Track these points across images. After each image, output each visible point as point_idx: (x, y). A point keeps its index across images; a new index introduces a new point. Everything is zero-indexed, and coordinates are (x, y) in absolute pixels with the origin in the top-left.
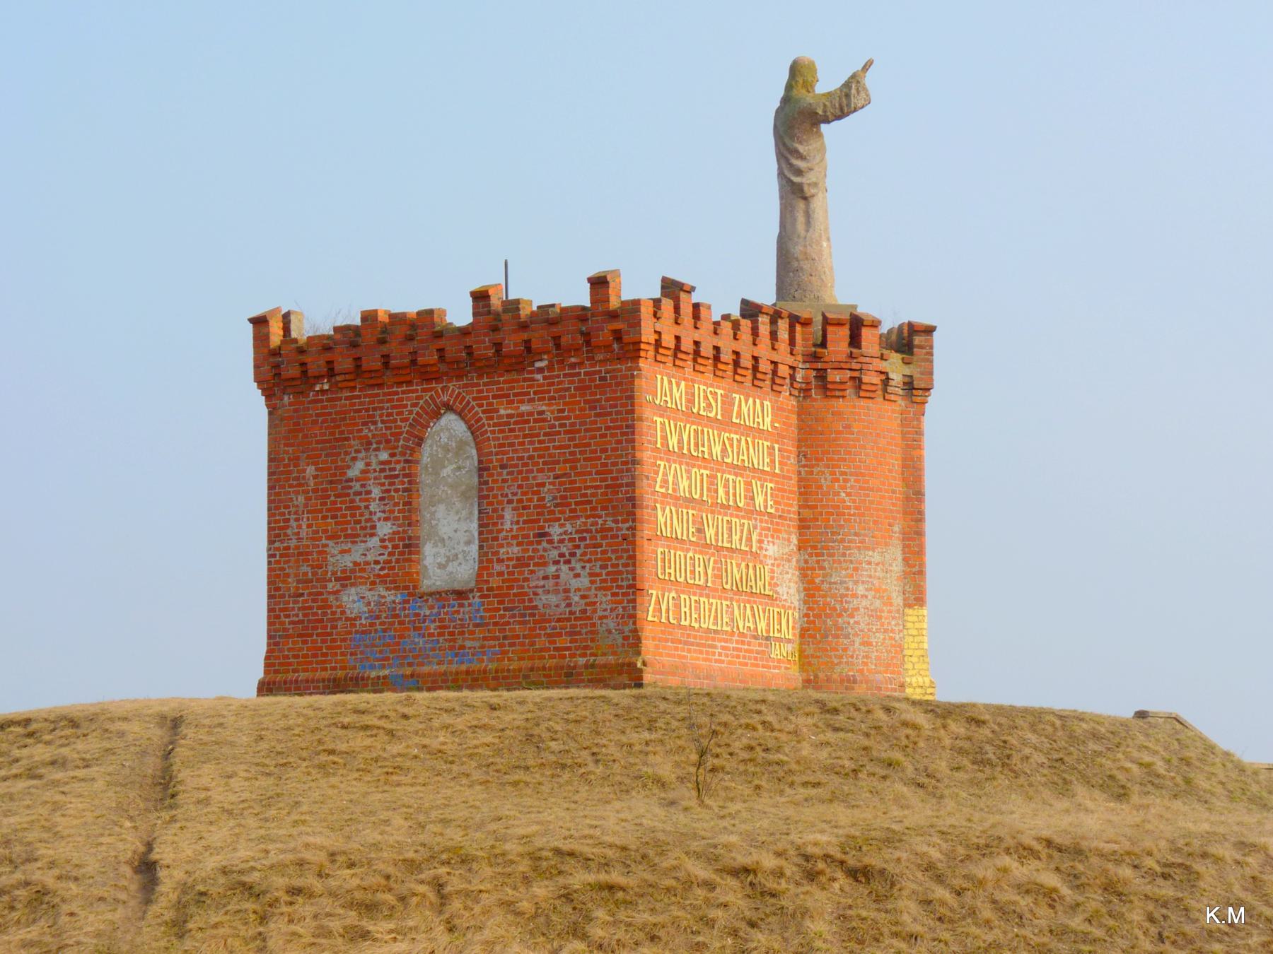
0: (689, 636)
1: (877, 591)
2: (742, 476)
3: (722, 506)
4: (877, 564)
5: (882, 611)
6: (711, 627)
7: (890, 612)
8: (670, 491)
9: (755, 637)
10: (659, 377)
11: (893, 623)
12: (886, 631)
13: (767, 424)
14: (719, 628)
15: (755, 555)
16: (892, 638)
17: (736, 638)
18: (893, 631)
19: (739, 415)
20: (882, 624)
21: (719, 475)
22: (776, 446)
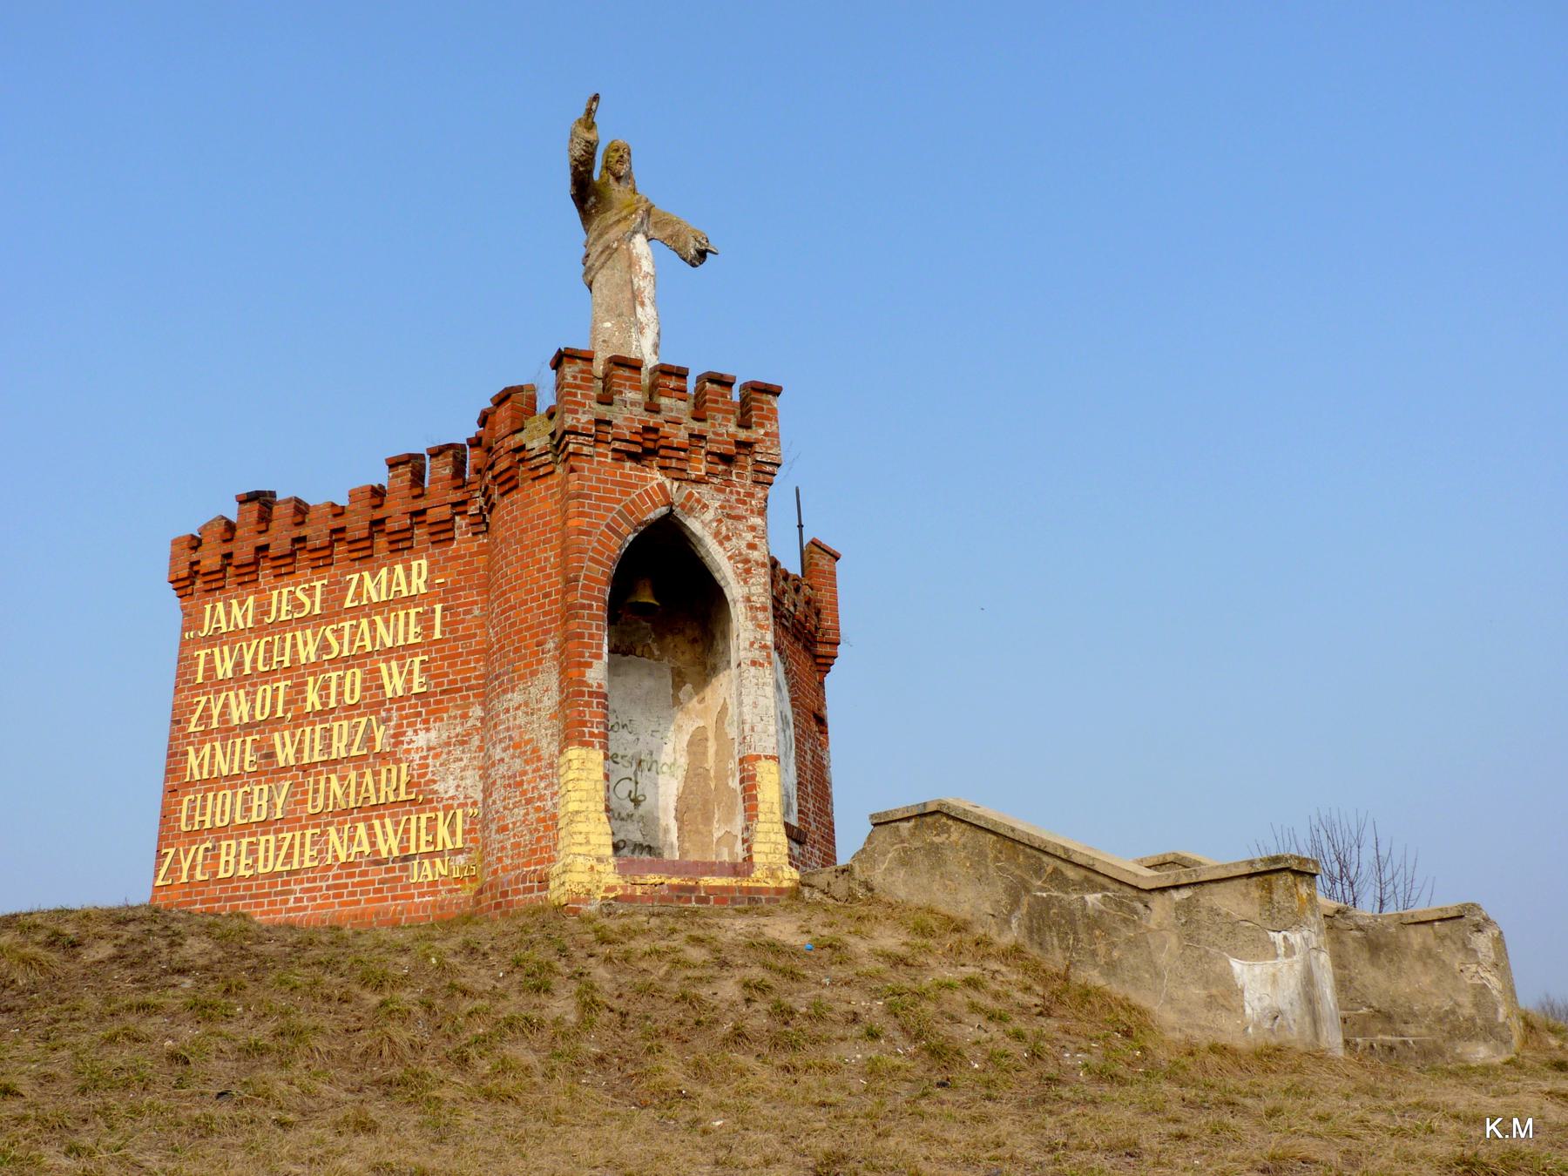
0: (237, 889)
1: (517, 746)
2: (360, 666)
3: (318, 713)
4: (517, 708)
5: (525, 773)
6: (278, 868)
7: (537, 770)
8: (215, 725)
9: (378, 863)
10: (208, 607)
11: (543, 785)
12: (529, 801)
13: (419, 585)
14: (296, 866)
15: (382, 756)
16: (538, 809)
17: (335, 871)
18: (541, 798)
19: (358, 595)
20: (524, 793)
21: (311, 679)
22: (438, 607)
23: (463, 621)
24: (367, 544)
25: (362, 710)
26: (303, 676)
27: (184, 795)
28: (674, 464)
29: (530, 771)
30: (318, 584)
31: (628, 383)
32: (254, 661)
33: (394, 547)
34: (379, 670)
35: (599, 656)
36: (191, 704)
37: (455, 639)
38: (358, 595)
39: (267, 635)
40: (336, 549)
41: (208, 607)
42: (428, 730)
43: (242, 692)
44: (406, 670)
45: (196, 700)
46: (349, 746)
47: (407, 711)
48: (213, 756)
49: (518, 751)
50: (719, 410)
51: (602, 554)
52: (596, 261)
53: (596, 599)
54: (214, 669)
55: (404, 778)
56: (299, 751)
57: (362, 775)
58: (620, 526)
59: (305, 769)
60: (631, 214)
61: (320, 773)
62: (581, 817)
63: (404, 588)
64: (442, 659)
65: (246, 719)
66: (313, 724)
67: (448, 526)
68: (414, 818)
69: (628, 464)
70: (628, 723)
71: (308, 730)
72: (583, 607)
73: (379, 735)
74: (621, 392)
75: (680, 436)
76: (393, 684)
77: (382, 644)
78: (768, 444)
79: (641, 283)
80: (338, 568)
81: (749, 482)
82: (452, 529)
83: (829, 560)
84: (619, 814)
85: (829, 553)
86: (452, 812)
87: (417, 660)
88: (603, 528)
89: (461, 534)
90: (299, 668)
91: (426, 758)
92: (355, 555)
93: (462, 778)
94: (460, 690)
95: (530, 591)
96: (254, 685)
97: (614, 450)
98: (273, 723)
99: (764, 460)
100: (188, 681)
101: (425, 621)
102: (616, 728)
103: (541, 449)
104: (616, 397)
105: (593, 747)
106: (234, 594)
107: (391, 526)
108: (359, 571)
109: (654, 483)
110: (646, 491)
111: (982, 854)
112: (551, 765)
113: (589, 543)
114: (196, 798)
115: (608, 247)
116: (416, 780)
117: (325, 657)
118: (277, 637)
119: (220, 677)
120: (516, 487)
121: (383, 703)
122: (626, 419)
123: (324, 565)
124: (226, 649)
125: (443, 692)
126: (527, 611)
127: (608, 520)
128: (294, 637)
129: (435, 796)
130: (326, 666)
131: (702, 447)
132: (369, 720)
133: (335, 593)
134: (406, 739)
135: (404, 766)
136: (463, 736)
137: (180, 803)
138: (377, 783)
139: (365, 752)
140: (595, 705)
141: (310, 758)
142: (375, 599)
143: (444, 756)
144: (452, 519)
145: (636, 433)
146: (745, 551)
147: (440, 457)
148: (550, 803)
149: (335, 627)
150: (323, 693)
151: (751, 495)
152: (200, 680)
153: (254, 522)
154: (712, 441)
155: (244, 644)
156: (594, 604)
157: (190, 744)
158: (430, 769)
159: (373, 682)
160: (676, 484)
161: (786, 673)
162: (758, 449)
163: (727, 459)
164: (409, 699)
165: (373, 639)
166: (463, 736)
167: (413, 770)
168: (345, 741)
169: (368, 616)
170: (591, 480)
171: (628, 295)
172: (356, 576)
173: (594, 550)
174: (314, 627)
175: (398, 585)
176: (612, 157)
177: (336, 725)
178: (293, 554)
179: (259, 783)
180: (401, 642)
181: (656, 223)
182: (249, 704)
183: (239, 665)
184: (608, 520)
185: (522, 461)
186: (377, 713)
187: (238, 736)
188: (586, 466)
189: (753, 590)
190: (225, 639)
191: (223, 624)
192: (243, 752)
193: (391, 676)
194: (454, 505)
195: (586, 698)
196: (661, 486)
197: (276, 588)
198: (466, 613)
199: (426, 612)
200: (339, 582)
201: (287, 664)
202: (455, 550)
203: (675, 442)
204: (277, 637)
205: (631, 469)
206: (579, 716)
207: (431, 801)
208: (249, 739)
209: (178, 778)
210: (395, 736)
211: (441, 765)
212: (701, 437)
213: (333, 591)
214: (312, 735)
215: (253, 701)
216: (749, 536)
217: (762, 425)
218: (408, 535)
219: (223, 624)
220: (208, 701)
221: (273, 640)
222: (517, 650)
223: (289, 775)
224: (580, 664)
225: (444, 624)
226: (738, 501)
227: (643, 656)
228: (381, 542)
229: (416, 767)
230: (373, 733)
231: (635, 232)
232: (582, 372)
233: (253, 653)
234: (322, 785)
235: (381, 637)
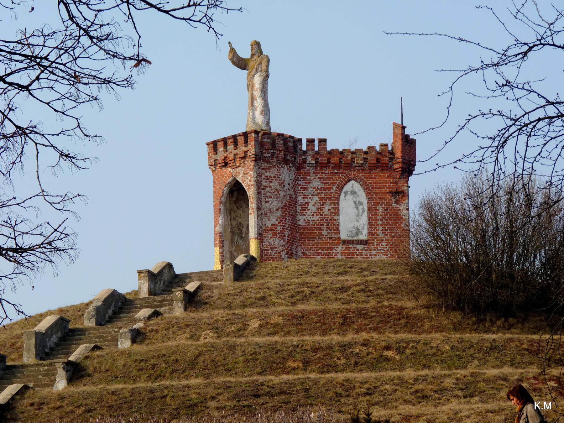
51: (218, 196)
69: (223, 169)
151: (250, 165)
161: (361, 185)
162: (249, 152)
163: (244, 158)
196: (230, 172)
216: (249, 178)
226: (247, 169)
231: (254, 76)
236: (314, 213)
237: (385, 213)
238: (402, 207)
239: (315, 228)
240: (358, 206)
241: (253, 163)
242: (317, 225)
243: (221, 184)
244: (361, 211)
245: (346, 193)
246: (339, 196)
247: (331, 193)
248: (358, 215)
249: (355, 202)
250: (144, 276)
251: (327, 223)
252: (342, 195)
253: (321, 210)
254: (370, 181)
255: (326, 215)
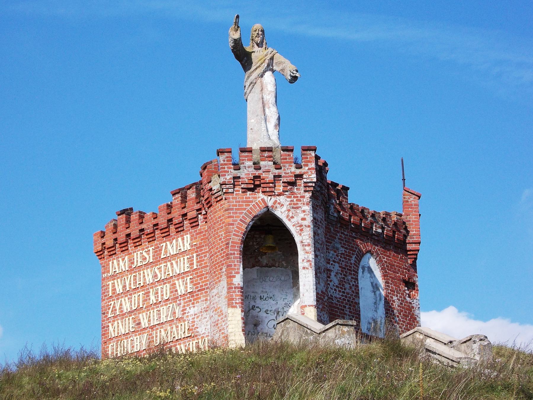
2: (169, 282)
4: (215, 295)
5: (218, 320)
10: (111, 262)
11: (224, 324)
13: (187, 247)
16: (223, 333)
19: (166, 252)
20: (219, 328)
21: (151, 290)
22: (195, 255)
23: (204, 260)
24: (167, 230)
25: (171, 301)
26: (148, 289)
27: (110, 343)
28: (268, 190)
29: (220, 319)
30: (151, 249)
31: (246, 158)
32: (130, 284)
33: (177, 230)
34: (175, 284)
35: (238, 273)
36: (108, 305)
37: (202, 268)
38: (166, 252)
39: (134, 273)
40: (156, 233)
41: (111, 262)
42: (194, 307)
43: (126, 298)
44: (185, 283)
45: (110, 303)
46: (167, 316)
47: (186, 300)
48: (118, 326)
49: (216, 312)
50: (287, 162)
51: (238, 232)
52: (247, 90)
53: (236, 250)
54: (115, 289)
55: (187, 328)
56: (149, 321)
57: (172, 328)
58: (246, 219)
59: (152, 328)
60: (262, 64)
61: (157, 329)
62: (233, 334)
63: (182, 248)
64: (198, 277)
65: (129, 310)
66: (153, 309)
67: (196, 220)
68: (191, 343)
69: (249, 193)
70: (272, 296)
71: (152, 311)
72: (231, 254)
73: (177, 311)
74: (244, 163)
75: (270, 177)
76: (181, 289)
77: (176, 272)
78: (310, 173)
79: (267, 97)
80: (158, 241)
81: (302, 191)
82: (197, 221)
83: (414, 198)
84: (270, 335)
85: (414, 194)
86: (204, 339)
87: (188, 278)
88: (239, 221)
89: (201, 223)
90: (146, 286)
91: (194, 318)
92: (163, 235)
93: (207, 325)
94: (204, 289)
95: (217, 249)
96: (131, 295)
97: (242, 188)
98: (139, 310)
99: (308, 181)
100: (106, 296)
101: (190, 260)
102: (267, 299)
103: (217, 190)
104: (242, 166)
105: (236, 307)
106: (120, 256)
107: (175, 221)
108: (165, 242)
109: (260, 199)
110: (257, 203)
111: (295, 329)
112: (226, 316)
113: (233, 228)
114: (114, 344)
115: (251, 83)
116: (191, 328)
117: (156, 280)
118: (137, 273)
119: (118, 293)
120: (211, 205)
121: (178, 297)
122: (246, 174)
123: (152, 241)
124: (119, 280)
125: (198, 291)
126: (217, 256)
127: (241, 218)
128: (144, 273)
129: (198, 334)
130: (157, 284)
131: (281, 180)
132: (173, 305)
133: (157, 251)
134: (186, 311)
135: (186, 323)
136: (206, 308)
137: (108, 347)
138: (177, 330)
139: (172, 319)
140: (237, 292)
141: (153, 323)
142: (172, 254)
143: (200, 317)
144: (197, 217)
145: (250, 179)
146: (300, 222)
147: (191, 189)
148: (226, 330)
149: (158, 267)
150: (156, 295)
151: (303, 197)
152: (110, 295)
153: (125, 224)
154: (284, 177)
155: (126, 278)
156: (235, 252)
157: (109, 322)
158: (196, 323)
159: (174, 289)
160: (269, 198)
162: (304, 176)
164: (187, 295)
165: (173, 270)
166: (206, 308)
167: (190, 324)
168: (165, 315)
169: (170, 261)
170: (233, 202)
171: (261, 105)
172: (164, 244)
173: (235, 231)
174: (151, 268)
175: (180, 246)
176: (254, 34)
177: (161, 308)
178: (140, 237)
179: (136, 335)
180: (182, 271)
181: (276, 63)
182: (130, 303)
183: (124, 286)
184: (241, 218)
185: (213, 195)
186: (176, 302)
187: (127, 317)
188: (231, 196)
189: (304, 238)
190: (118, 276)
191: (117, 270)
192: (129, 323)
193: (180, 286)
194: (198, 210)
195: (234, 289)
196: (263, 200)
197: (135, 252)
198: (205, 256)
199: (190, 258)
200: (158, 247)
201: (142, 285)
202: (201, 229)
203: (267, 180)
204: (137, 273)
205: (250, 195)
206: (231, 296)
207: (197, 336)
208: (131, 318)
209: (106, 337)
210: (183, 311)
211: (199, 321)
212: (280, 176)
213: (156, 251)
214: (153, 313)
215: (131, 301)
217: (307, 165)
218: (181, 225)
219: (117, 270)
220: (114, 303)
221: (136, 275)
222: (215, 272)
223: (146, 331)
224: (230, 277)
225: (198, 262)
227: (279, 267)
228: (172, 228)
229: (191, 323)
230: (175, 310)
231: (264, 72)
232: (227, 157)
233: (129, 281)
234: (158, 334)
235: (175, 270)
236: (337, 286)
237: (400, 306)
238: (415, 303)
239: (338, 308)
240: (375, 290)
241: (308, 195)
242: (340, 305)
243: (243, 215)
244: (378, 299)
245: (363, 268)
246: (358, 270)
247: (351, 264)
248: (375, 303)
249: (372, 283)
250: (348, 331)
251: (350, 305)
252: (360, 270)
253: (343, 285)
254: (385, 260)
255: (348, 294)
